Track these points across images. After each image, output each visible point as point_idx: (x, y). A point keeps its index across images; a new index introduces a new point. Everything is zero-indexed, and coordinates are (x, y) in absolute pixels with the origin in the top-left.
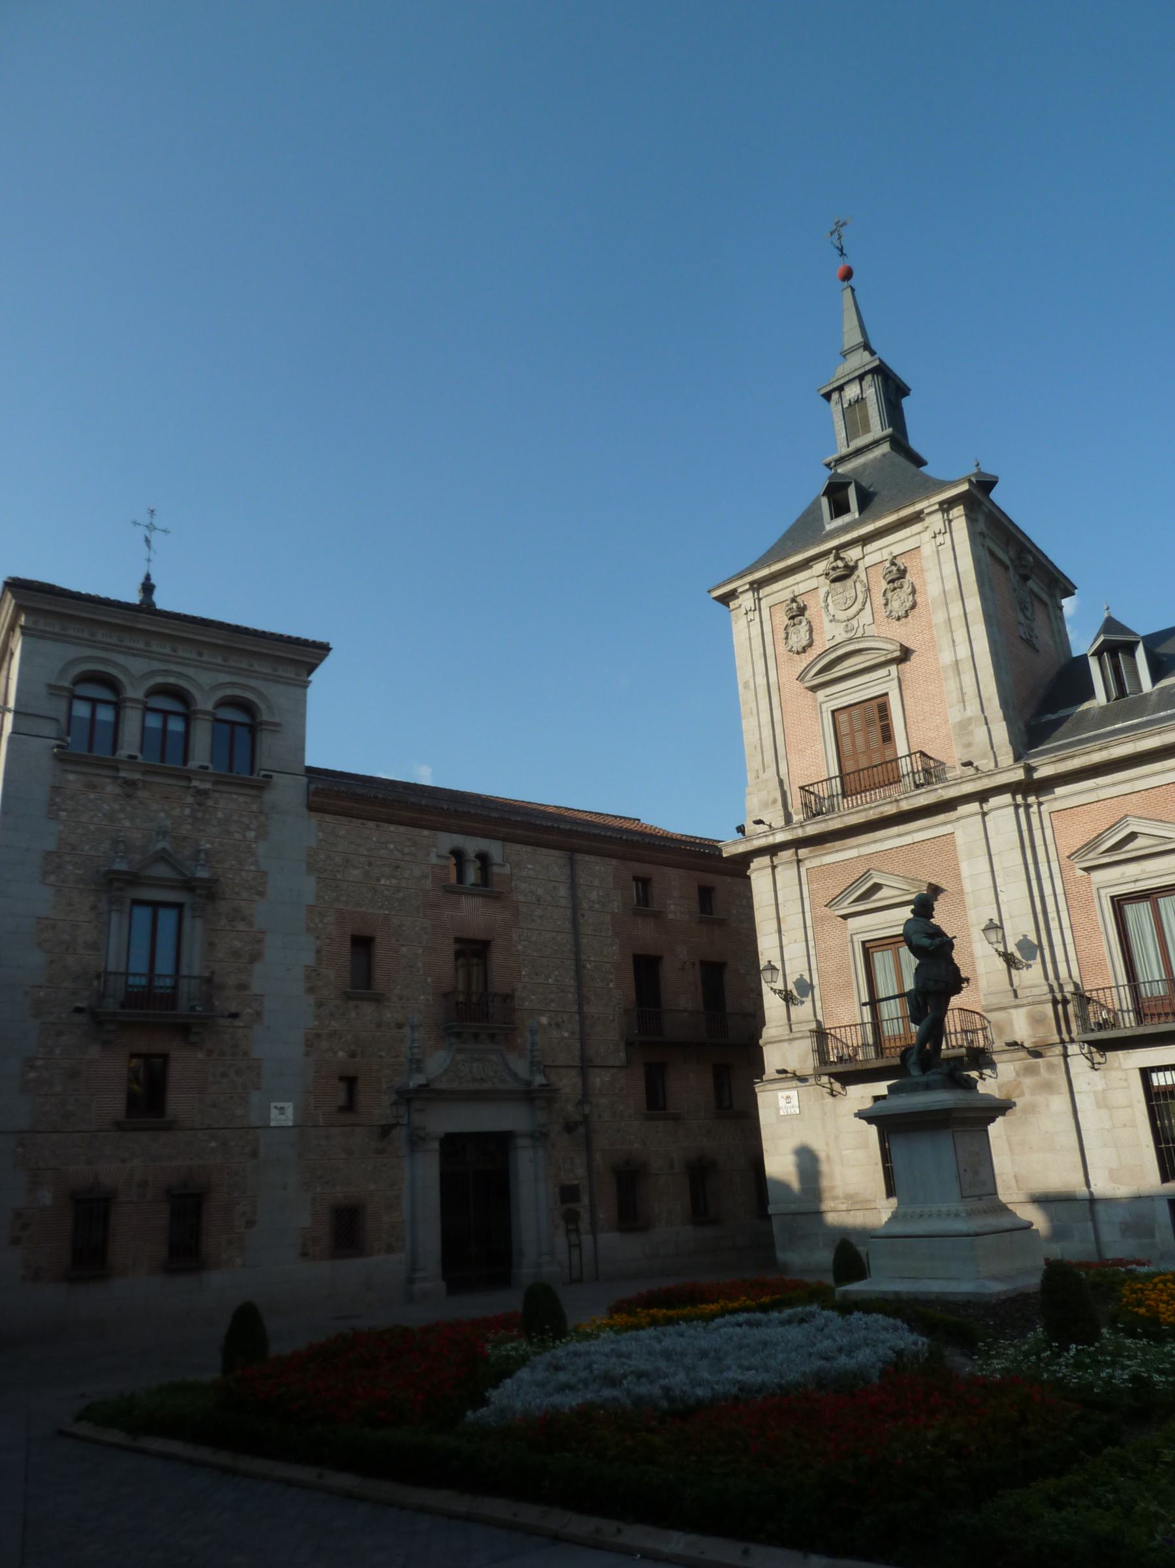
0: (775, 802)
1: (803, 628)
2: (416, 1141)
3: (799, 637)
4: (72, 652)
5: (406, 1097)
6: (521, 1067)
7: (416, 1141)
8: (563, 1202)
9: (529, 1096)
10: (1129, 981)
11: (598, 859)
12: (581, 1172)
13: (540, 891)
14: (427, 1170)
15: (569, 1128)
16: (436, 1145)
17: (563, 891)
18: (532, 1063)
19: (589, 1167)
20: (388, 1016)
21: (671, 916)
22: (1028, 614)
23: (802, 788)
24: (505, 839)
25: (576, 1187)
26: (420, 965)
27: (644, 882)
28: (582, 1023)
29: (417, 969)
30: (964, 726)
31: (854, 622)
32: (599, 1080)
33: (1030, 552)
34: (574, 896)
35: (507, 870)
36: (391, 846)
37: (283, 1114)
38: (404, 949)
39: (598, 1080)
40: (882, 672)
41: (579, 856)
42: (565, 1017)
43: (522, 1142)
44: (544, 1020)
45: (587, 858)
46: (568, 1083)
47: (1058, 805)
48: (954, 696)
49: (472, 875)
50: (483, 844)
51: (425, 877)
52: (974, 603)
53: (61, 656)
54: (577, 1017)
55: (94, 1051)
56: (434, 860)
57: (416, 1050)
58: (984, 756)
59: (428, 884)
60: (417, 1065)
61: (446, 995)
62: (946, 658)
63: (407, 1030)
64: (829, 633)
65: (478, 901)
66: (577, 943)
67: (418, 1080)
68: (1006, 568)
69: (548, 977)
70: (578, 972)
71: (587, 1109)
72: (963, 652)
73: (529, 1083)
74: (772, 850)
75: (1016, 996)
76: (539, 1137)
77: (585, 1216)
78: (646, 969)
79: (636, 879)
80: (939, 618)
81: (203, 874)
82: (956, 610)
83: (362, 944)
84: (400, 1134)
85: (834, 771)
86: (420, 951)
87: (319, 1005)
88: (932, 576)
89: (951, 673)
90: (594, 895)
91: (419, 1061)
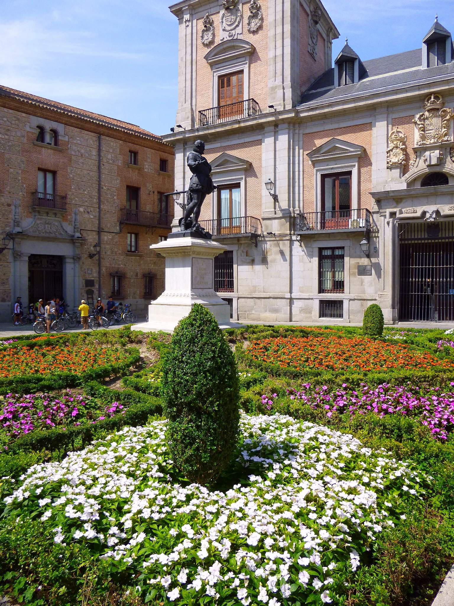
0: (188, 118)
1: (210, 33)
2: (17, 255)
3: (208, 37)
6: (69, 229)
7: (17, 255)
8: (87, 286)
9: (72, 240)
10: (322, 210)
11: (113, 140)
12: (95, 275)
13: (83, 151)
15: (91, 256)
16: (27, 259)
17: (94, 153)
18: (75, 228)
19: (99, 273)
21: (146, 170)
22: (314, 41)
23: (200, 112)
25: (93, 280)
26: (20, 178)
27: (134, 154)
28: (99, 212)
30: (273, 89)
31: (233, 32)
32: (106, 237)
33: (321, 10)
34: (99, 155)
35: (66, 139)
36: (5, 119)
38: (12, 170)
39: (106, 238)
40: (243, 59)
41: (102, 137)
42: (92, 209)
43: (68, 260)
44: (82, 209)
45: (107, 138)
46: (91, 238)
47: (307, 131)
48: (272, 73)
51: (24, 136)
52: (288, 27)
54: (98, 210)
56: (28, 129)
57: (17, 217)
58: (280, 104)
59: (25, 140)
60: (17, 223)
62: (271, 54)
63: (13, 207)
64: (221, 36)
65: (51, 152)
66: (99, 177)
67: (19, 229)
68: (308, 15)
69: (84, 191)
70: (99, 190)
71: (98, 249)
72: (279, 52)
73: (73, 236)
75: (275, 213)
76: (76, 259)
77: (96, 292)
78: (133, 192)
79: (131, 152)
80: (271, 33)
82: (279, 30)
85: (216, 105)
86: (20, 172)
88: (271, 11)
89: (272, 62)
90: (109, 156)
91: (19, 222)
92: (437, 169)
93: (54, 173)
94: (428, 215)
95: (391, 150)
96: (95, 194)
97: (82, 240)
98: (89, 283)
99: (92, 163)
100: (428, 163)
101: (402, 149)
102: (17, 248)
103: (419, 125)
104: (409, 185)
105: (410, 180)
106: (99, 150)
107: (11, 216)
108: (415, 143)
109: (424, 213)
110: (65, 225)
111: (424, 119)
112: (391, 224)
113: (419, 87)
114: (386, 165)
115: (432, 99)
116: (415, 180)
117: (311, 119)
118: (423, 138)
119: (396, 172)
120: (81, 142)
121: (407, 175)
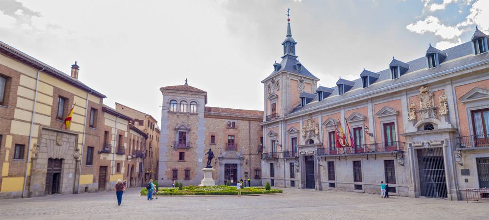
2: (221, 164)
4: (170, 97)
5: (219, 158)
14: (223, 169)
17: (248, 127)
19: (250, 169)
20: (217, 147)
24: (238, 120)
29: (221, 141)
32: (252, 156)
37: (200, 160)
43: (238, 165)
49: (231, 126)
50: (234, 121)
53: (169, 98)
55: (175, 152)
60: (221, 154)
61: (226, 144)
67: (221, 156)
74: (265, 125)
81: (188, 128)
83: (213, 137)
84: (218, 164)
87: (206, 145)
93: (234, 136)
96: (248, 142)
97: (243, 159)
98: (246, 173)
99: (247, 131)
102: (221, 162)
106: (250, 126)
107: (219, 152)
110: (237, 153)
117: (289, 119)
120: (242, 125)
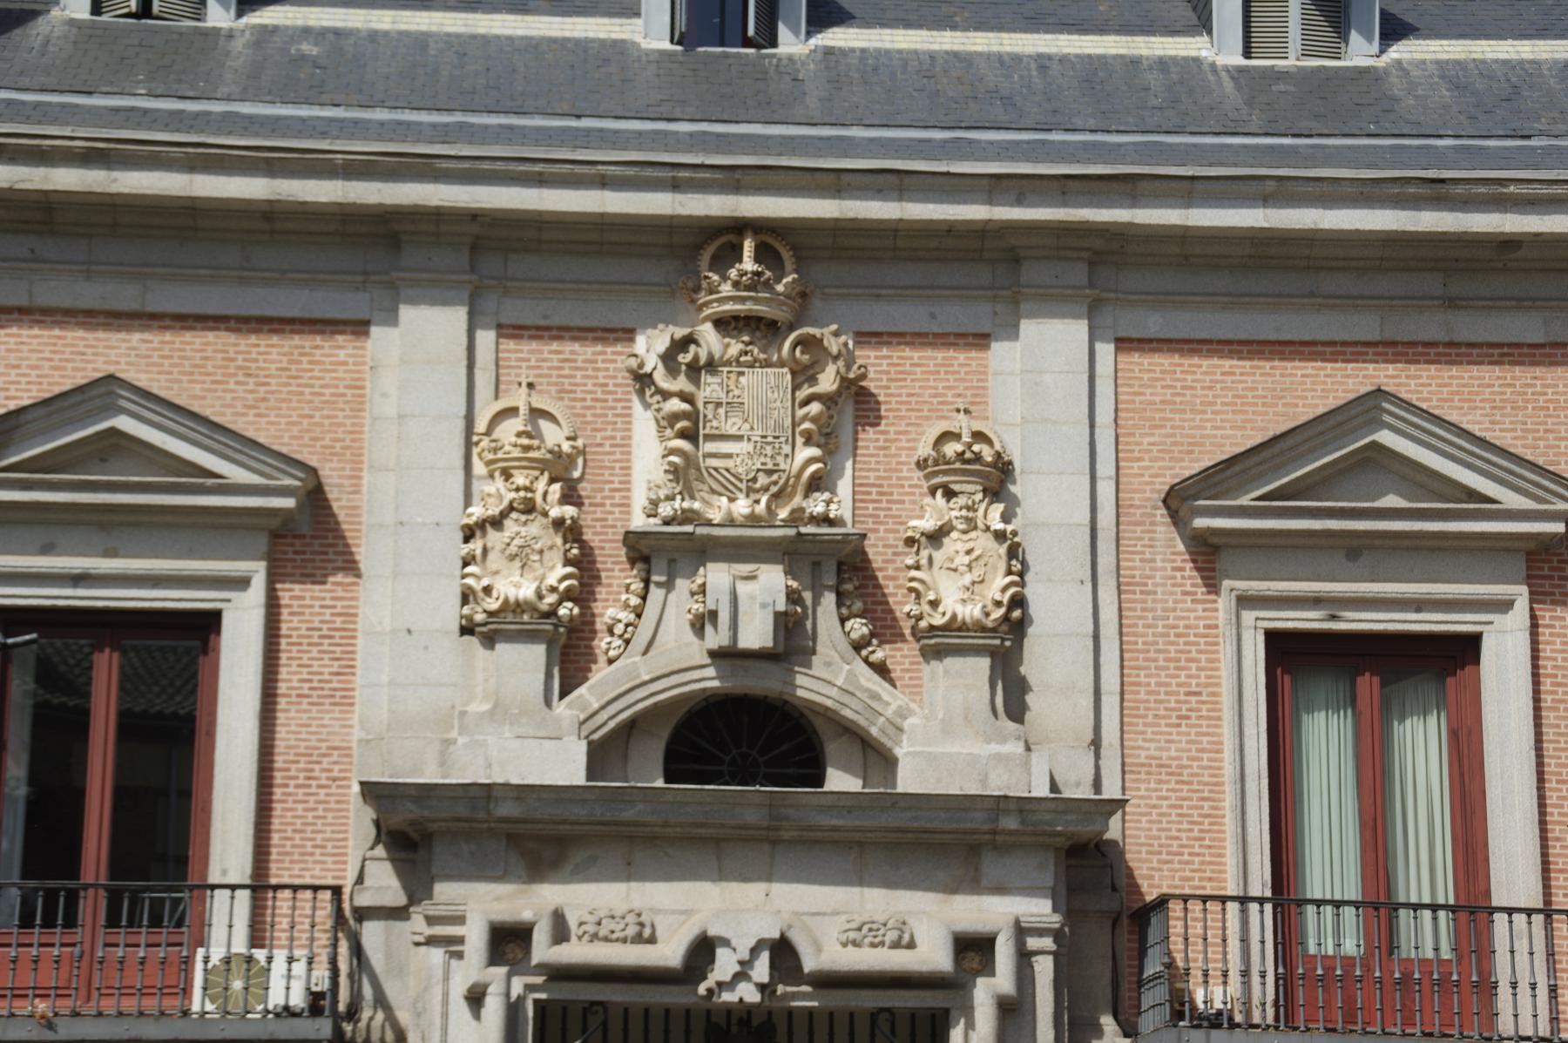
92: (761, 682)
94: (725, 965)
95: (497, 523)
100: (716, 638)
101: (558, 523)
103: (666, 395)
104: (606, 752)
105: (609, 722)
108: (639, 500)
109: (703, 949)
111: (694, 370)
112: (494, 1007)
113: (676, 179)
114: (450, 613)
115: (748, 264)
116: (631, 729)
118: (684, 474)
119: (526, 663)
121: (588, 694)
